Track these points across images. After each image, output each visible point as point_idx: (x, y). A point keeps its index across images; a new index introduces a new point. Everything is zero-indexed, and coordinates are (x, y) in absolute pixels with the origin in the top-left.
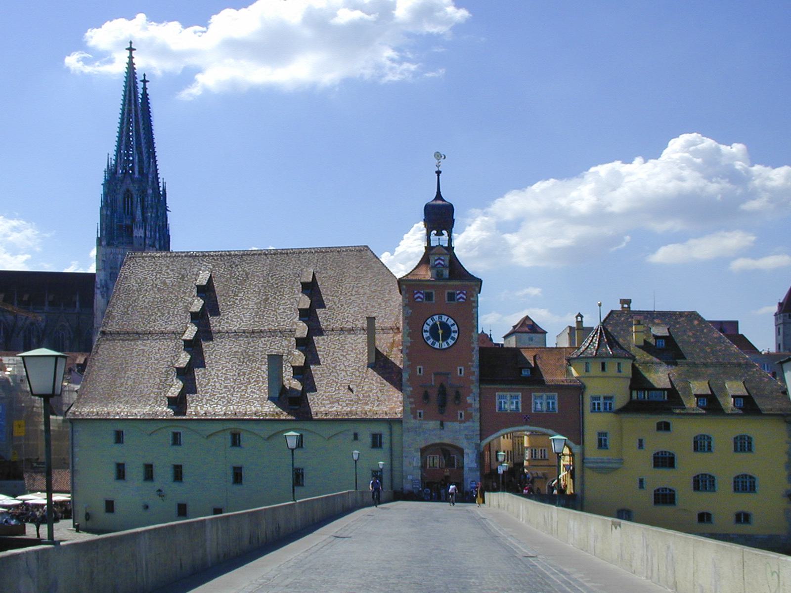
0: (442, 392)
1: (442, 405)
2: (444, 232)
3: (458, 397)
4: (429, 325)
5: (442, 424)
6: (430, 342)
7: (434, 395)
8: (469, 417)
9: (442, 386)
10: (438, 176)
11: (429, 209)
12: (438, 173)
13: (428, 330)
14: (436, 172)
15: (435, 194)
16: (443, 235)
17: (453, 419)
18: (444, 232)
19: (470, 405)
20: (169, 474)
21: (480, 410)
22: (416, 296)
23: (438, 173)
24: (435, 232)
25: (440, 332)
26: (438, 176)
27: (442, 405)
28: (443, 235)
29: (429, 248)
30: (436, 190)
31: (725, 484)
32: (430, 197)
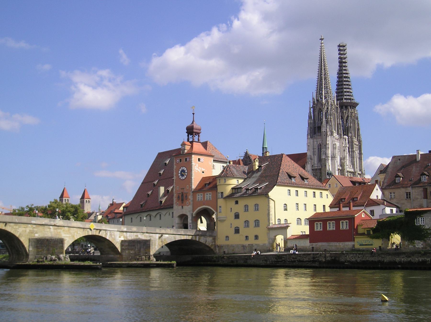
0: (182, 195)
1: (182, 200)
3: (186, 196)
5: (182, 207)
6: (180, 177)
7: (180, 195)
8: (190, 204)
9: (182, 193)
10: (193, 115)
12: (193, 114)
14: (193, 113)
17: (186, 205)
19: (190, 199)
20: (253, 238)
21: (193, 201)
22: (177, 161)
23: (193, 114)
26: (193, 115)
27: (182, 200)
31: (252, 224)
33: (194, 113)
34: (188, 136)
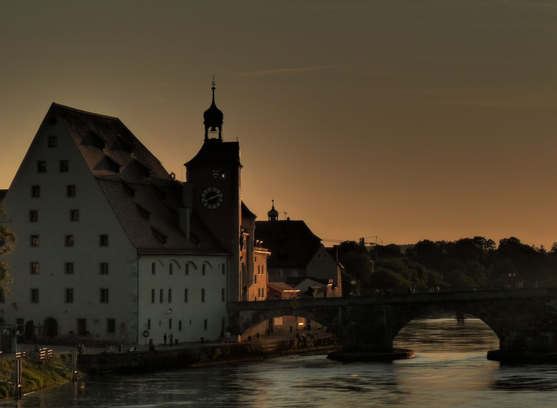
2: (217, 128)
4: (205, 194)
10: (213, 91)
11: (207, 115)
12: (213, 89)
13: (204, 197)
15: (211, 103)
16: (216, 131)
18: (217, 128)
23: (213, 89)
24: (210, 129)
25: (212, 198)
26: (213, 91)
28: (216, 131)
29: (206, 139)
30: (212, 101)
32: (208, 107)
33: (215, 86)
34: (206, 129)
